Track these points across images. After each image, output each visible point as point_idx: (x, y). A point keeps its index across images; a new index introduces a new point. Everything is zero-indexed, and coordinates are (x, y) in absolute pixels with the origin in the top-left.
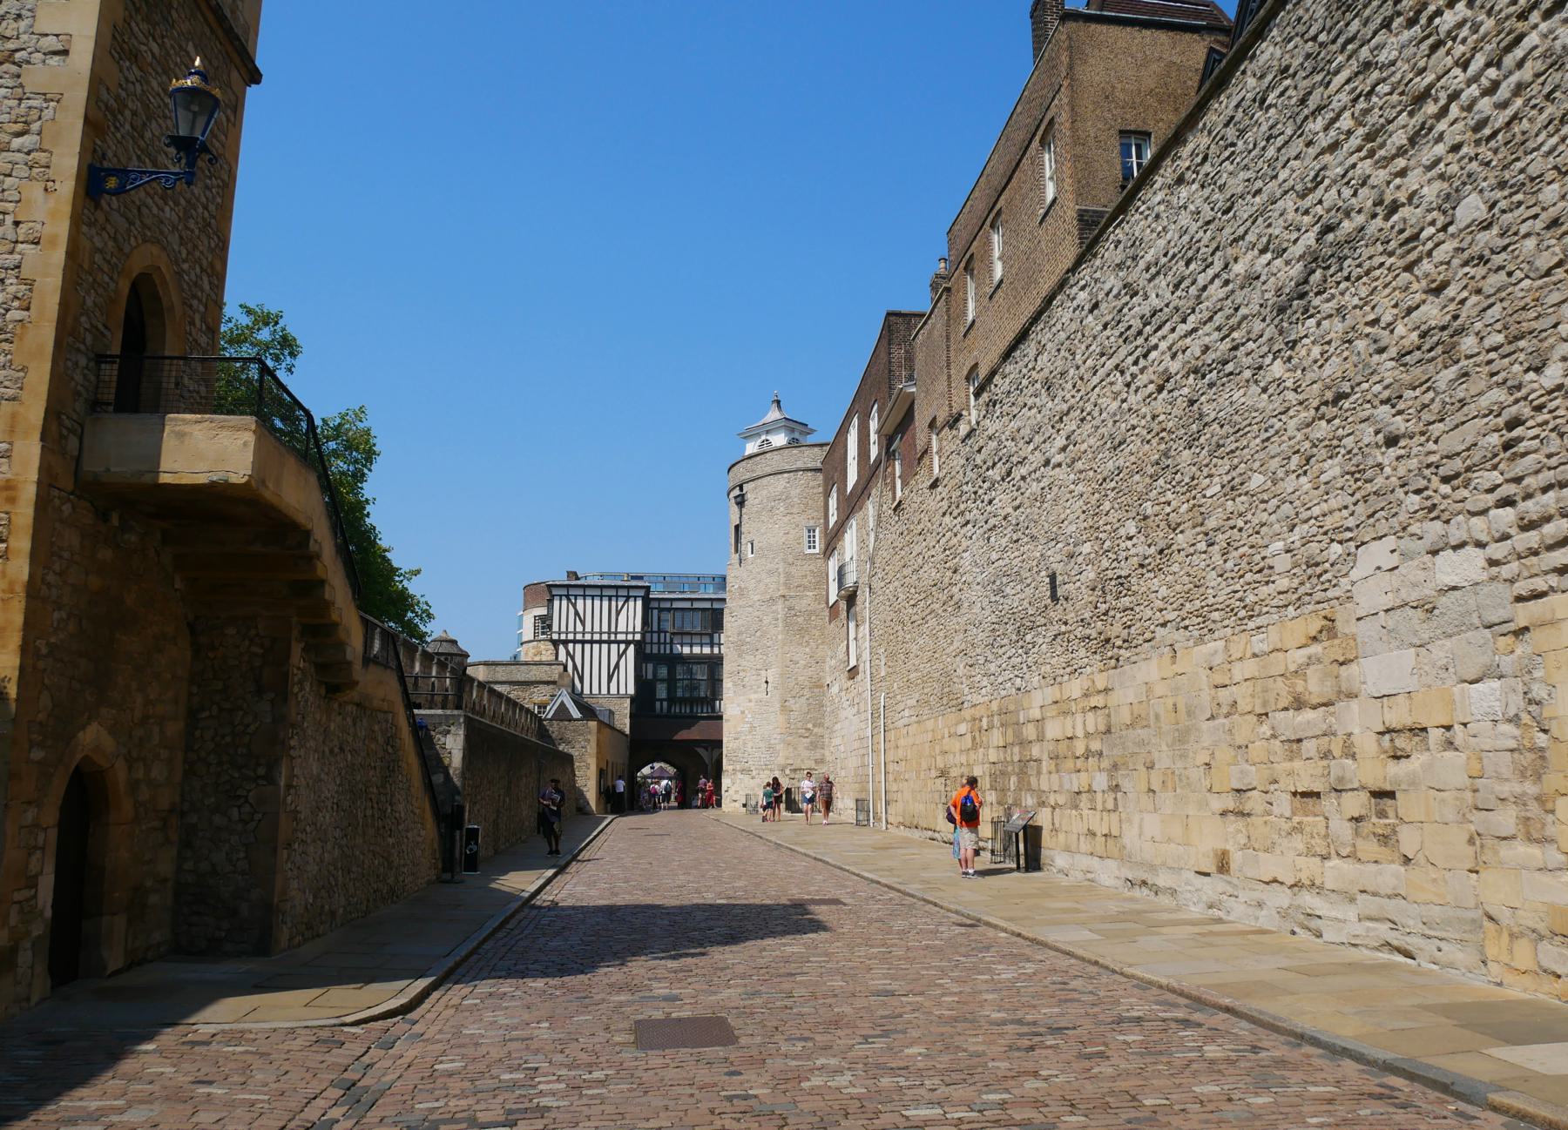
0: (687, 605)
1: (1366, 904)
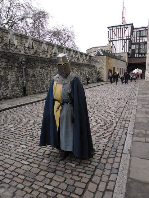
0: (144, 29)
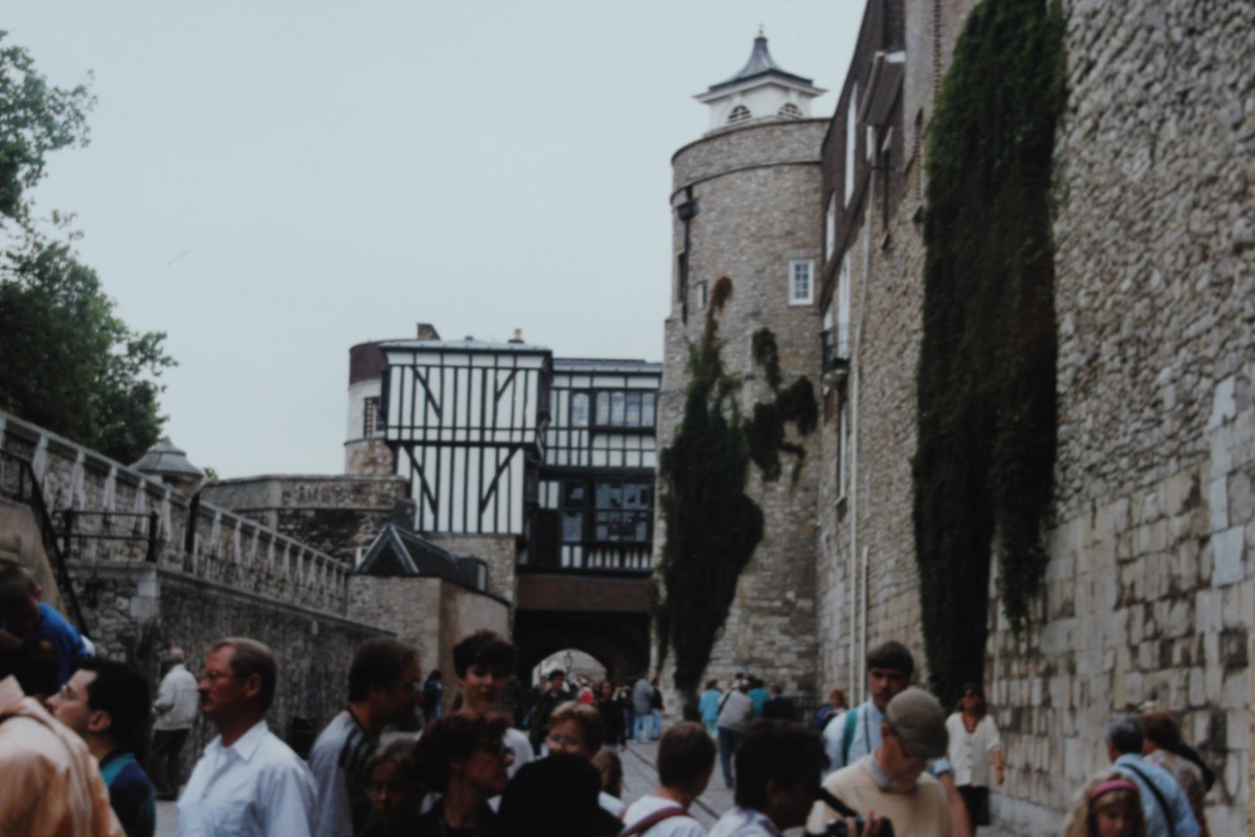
0: (618, 383)
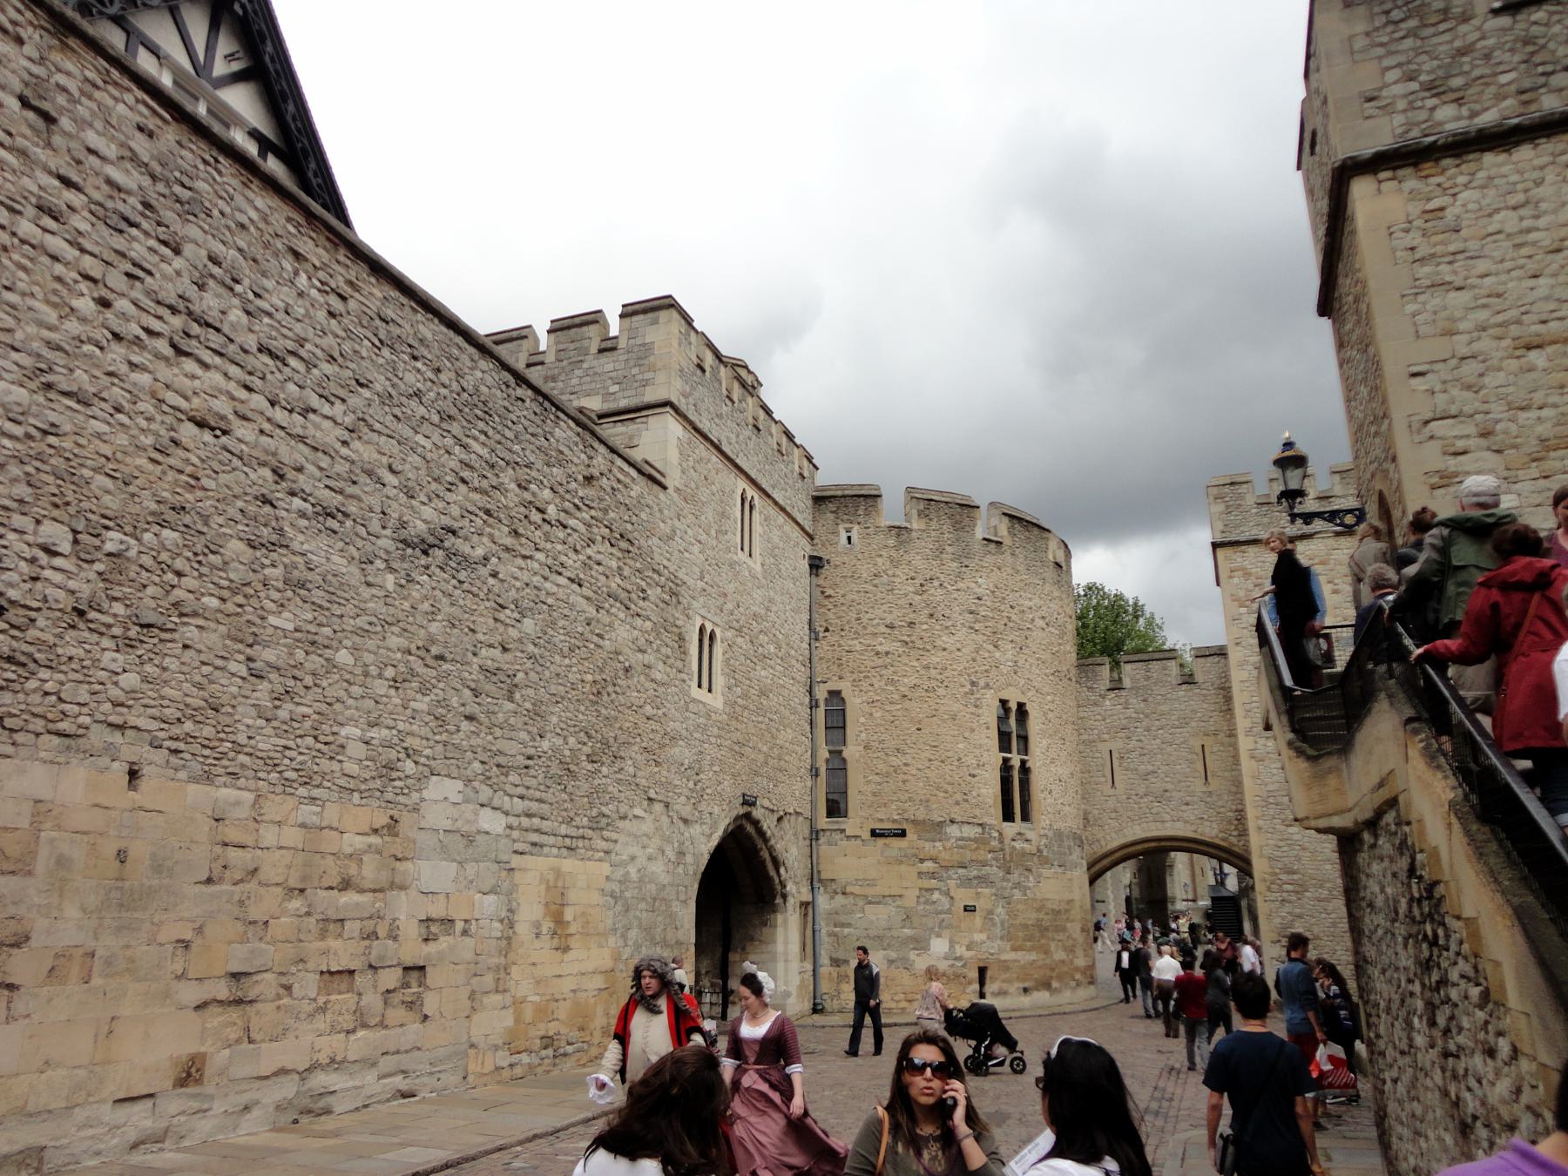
1: (386, 1064)
